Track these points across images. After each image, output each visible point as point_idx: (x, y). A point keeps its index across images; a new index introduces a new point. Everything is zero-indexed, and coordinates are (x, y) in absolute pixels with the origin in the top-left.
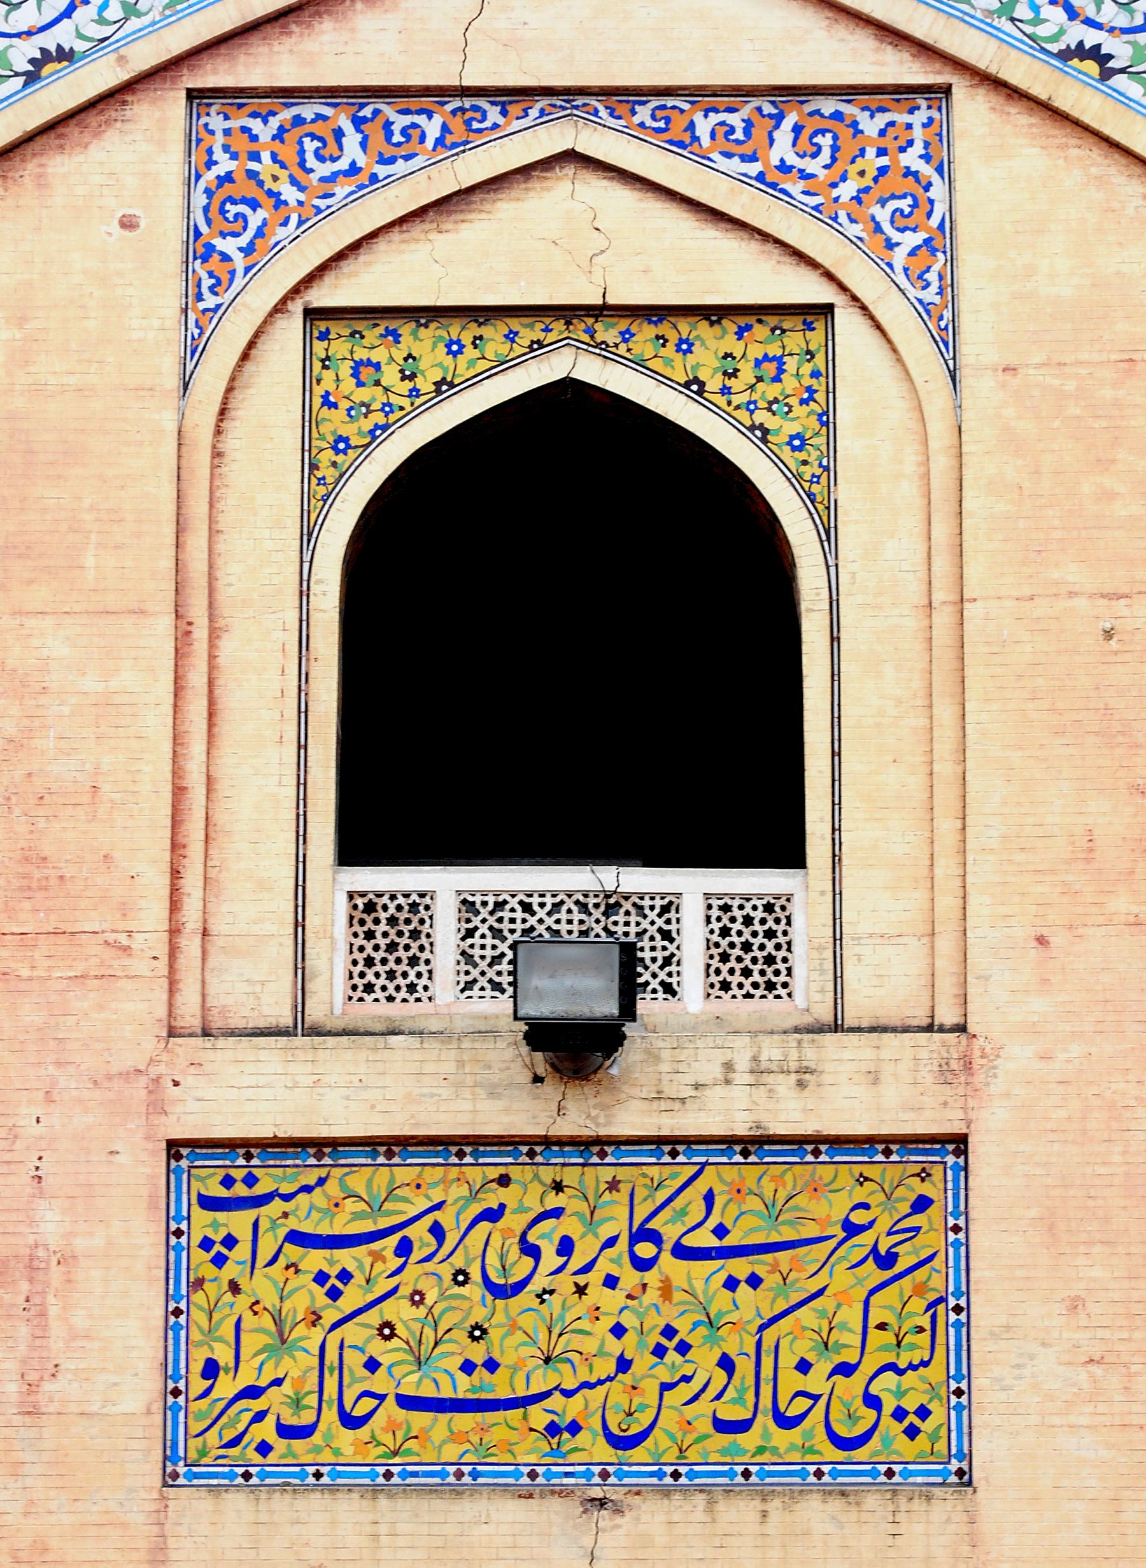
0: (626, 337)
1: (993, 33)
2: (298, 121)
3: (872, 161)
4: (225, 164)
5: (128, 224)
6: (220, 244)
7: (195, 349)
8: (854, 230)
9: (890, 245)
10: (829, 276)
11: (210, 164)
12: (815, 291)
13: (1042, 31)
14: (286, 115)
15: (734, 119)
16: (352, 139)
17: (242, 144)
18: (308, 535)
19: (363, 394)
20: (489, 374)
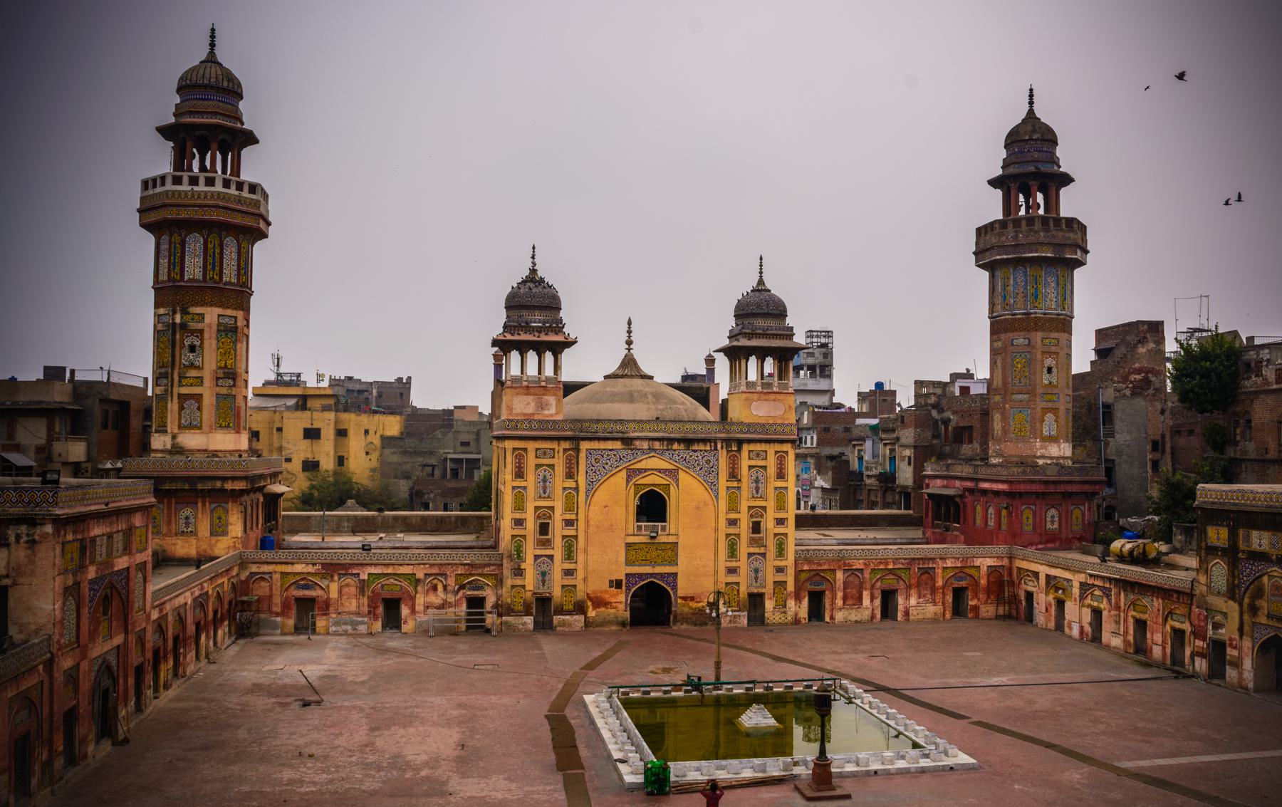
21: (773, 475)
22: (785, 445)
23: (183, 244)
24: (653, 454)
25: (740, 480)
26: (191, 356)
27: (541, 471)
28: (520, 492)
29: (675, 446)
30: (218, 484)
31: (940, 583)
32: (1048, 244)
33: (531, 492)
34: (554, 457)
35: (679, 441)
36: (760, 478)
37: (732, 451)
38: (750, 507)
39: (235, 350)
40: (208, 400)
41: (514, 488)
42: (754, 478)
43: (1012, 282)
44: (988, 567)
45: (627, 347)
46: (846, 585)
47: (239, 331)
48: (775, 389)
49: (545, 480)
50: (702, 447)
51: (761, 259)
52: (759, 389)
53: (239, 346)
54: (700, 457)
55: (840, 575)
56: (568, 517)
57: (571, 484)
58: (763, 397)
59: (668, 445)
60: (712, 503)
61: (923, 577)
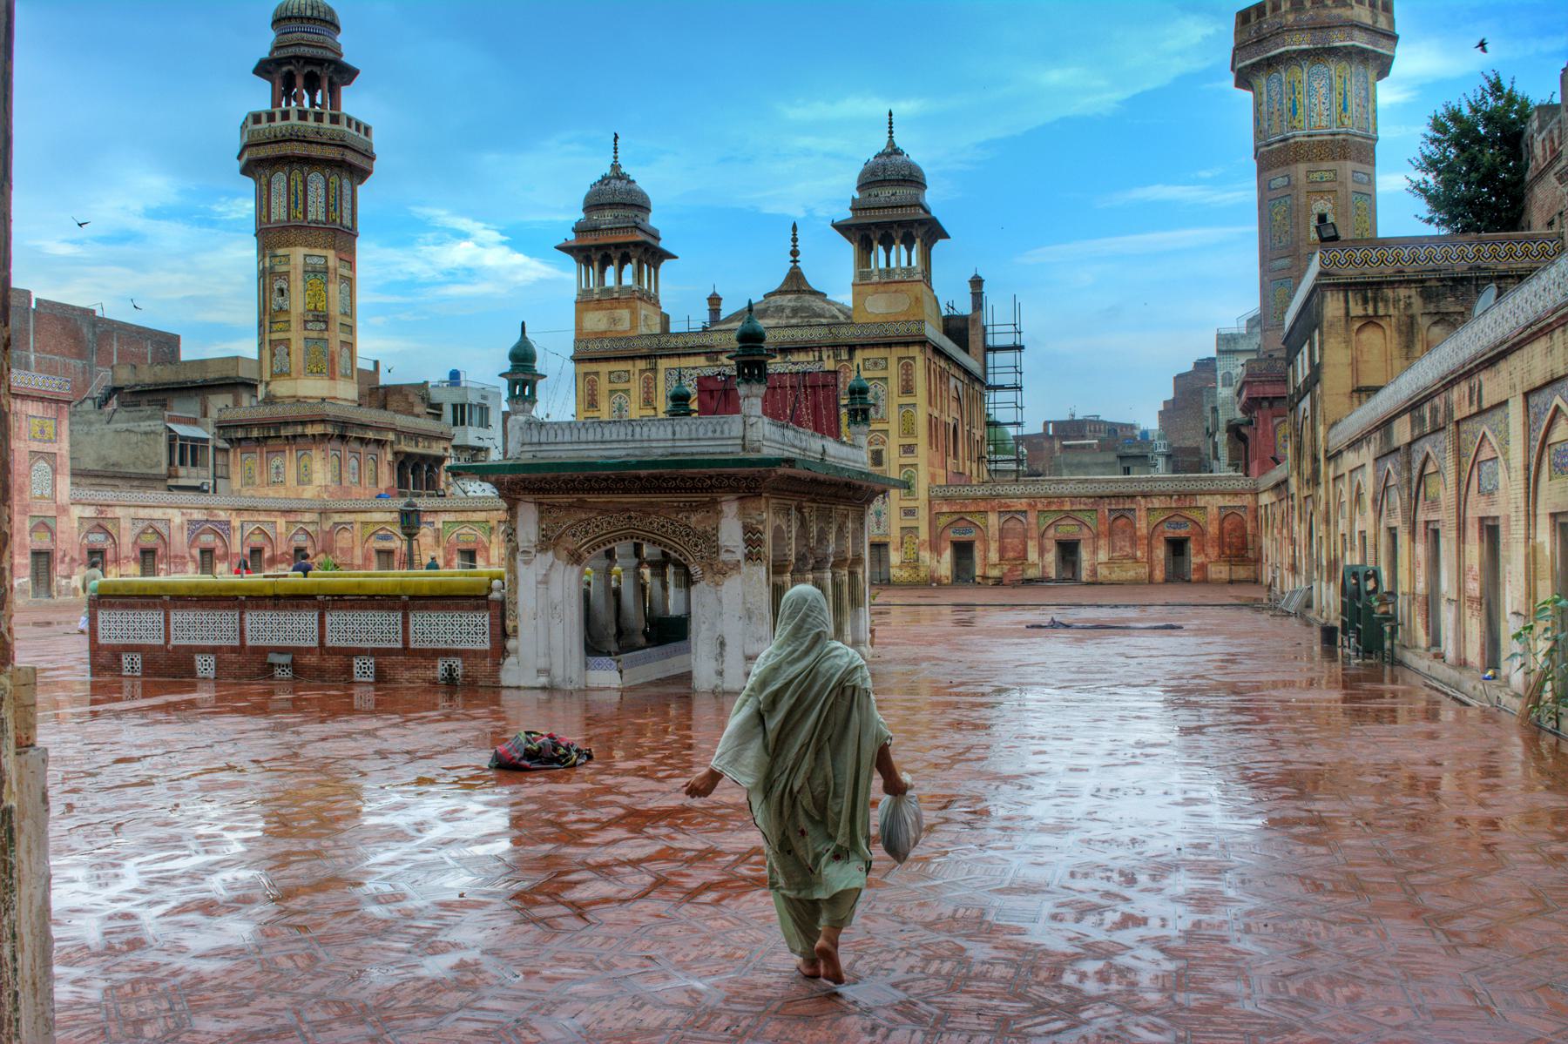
21: (895, 389)
23: (269, 184)
26: (280, 299)
30: (299, 429)
31: (1142, 527)
32: (1301, 29)
36: (880, 393)
37: (841, 361)
39: (327, 292)
40: (297, 344)
43: (1265, 99)
44: (1220, 508)
46: (1002, 532)
47: (331, 270)
48: (897, 278)
51: (890, 114)
52: (875, 279)
53: (331, 287)
55: (993, 520)
58: (881, 289)
61: (1119, 522)
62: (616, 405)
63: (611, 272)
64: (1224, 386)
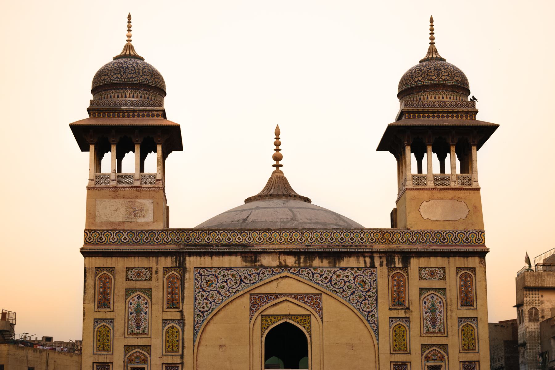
0: (291, 317)
1: (326, 289)
2: (260, 296)
3: (315, 301)
4: (253, 301)
5: (245, 307)
6: (253, 309)
7: (251, 319)
8: (313, 307)
9: (316, 309)
10: (310, 312)
11: (252, 301)
12: (309, 313)
13: (331, 289)
14: (259, 296)
15: (302, 296)
16: (265, 298)
17: (255, 299)
18: (262, 337)
19: (266, 323)
20: (278, 321)
21: (454, 301)
22: (470, 259)
24: (285, 274)
25: (408, 309)
27: (134, 298)
28: (104, 327)
29: (316, 262)
33: (119, 326)
34: (150, 279)
35: (322, 255)
36: (437, 305)
38: (424, 346)
41: (96, 321)
42: (428, 305)
45: (275, 163)
48: (453, 185)
49: (138, 310)
50: (351, 262)
51: (432, 21)
52: (431, 184)
54: (351, 277)
56: (170, 360)
57: (174, 314)
58: (437, 195)
59: (305, 261)
60: (369, 340)
62: (134, 307)
63: (108, 159)
64: (530, 320)
